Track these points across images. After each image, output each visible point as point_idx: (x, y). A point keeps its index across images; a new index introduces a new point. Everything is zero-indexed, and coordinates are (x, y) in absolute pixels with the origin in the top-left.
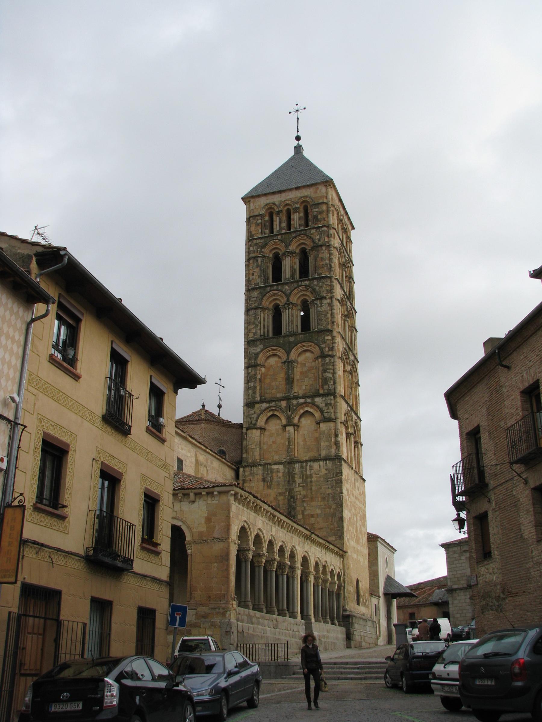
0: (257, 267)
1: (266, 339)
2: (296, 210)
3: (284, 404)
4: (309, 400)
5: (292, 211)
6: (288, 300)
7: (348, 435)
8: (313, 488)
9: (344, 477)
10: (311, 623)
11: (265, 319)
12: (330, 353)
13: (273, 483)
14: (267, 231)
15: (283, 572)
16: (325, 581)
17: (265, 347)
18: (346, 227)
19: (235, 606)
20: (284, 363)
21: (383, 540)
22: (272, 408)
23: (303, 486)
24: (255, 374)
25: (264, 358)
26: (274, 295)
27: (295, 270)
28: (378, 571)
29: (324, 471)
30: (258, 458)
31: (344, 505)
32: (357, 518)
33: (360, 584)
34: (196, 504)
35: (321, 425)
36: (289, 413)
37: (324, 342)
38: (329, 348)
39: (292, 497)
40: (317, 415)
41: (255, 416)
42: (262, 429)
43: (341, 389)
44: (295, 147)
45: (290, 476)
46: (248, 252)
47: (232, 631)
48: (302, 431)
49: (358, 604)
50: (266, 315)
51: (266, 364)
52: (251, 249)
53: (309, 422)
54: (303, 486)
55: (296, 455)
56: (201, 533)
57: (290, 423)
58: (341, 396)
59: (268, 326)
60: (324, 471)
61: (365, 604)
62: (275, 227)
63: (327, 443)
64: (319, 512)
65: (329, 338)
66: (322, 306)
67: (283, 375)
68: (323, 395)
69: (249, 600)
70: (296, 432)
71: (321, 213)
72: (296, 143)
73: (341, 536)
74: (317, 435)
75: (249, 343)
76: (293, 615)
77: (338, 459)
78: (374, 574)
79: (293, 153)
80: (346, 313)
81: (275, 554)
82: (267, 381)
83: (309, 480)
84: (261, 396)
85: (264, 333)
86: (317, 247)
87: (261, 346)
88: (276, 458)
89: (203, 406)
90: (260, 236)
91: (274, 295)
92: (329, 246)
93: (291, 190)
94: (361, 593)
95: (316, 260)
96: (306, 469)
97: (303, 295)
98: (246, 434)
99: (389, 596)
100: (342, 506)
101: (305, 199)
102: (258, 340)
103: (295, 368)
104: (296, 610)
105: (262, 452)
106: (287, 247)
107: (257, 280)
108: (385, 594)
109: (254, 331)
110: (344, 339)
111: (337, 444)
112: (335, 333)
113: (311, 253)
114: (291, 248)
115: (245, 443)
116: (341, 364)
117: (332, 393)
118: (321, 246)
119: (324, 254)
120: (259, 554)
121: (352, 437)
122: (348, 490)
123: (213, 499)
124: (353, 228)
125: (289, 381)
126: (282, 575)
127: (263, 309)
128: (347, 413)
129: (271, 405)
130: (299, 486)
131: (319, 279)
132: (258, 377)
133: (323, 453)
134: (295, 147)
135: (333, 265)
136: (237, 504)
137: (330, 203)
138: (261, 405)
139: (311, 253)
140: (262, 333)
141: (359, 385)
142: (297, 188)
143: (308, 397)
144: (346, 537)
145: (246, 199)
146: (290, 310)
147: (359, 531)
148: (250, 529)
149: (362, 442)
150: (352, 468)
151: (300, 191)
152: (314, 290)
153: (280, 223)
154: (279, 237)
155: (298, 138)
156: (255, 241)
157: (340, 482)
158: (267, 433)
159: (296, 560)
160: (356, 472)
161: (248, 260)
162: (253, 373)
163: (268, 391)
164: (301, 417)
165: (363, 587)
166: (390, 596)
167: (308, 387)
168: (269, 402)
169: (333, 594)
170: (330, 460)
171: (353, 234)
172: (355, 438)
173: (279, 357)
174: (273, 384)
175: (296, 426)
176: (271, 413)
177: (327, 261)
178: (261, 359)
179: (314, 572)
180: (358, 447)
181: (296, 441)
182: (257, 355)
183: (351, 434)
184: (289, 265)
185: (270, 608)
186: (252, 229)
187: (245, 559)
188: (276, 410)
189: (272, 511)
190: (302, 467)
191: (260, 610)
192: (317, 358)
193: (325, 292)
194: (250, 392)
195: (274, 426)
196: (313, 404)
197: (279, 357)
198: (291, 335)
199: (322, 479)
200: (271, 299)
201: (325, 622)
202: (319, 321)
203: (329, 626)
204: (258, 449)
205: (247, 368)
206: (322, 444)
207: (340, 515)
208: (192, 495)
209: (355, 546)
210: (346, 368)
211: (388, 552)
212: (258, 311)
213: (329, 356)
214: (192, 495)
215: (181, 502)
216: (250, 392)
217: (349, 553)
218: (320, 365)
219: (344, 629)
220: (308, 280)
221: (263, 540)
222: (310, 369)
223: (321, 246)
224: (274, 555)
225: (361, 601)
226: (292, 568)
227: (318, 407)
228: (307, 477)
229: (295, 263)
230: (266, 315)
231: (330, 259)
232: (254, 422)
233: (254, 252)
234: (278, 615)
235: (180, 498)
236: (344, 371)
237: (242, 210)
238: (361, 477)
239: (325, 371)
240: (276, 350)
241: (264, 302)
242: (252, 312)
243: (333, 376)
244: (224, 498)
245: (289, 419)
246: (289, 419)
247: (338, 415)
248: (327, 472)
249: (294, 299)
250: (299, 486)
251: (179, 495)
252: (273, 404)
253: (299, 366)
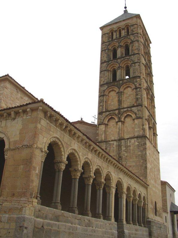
0: (105, 54)
1: (109, 83)
2: (123, 29)
3: (117, 112)
4: (129, 109)
5: (121, 30)
6: (119, 65)
7: (150, 128)
8: (131, 152)
9: (147, 146)
10: (123, 224)
11: (110, 75)
12: (139, 86)
13: (111, 150)
14: (110, 40)
15: (100, 188)
16: (134, 200)
17: (108, 87)
18: (147, 42)
19: (35, 204)
20: (117, 93)
21: (169, 184)
23: (126, 151)
25: (108, 92)
26: (113, 64)
27: (123, 53)
28: (166, 200)
29: (137, 143)
30: (103, 138)
31: (147, 160)
32: (155, 169)
33: (157, 205)
34: (16, 120)
35: (135, 120)
36: (119, 116)
37: (136, 82)
38: (139, 84)
39: (120, 157)
40: (134, 116)
41: (103, 118)
42: (106, 125)
43: (145, 103)
44: (124, 11)
45: (119, 146)
46: (102, 48)
47: (25, 226)
48: (126, 124)
49: (156, 215)
50: (109, 74)
51: (109, 95)
52: (103, 47)
53: (129, 120)
54: (126, 151)
55: (123, 136)
56: (15, 142)
57: (120, 121)
58: (145, 107)
59: (110, 78)
60: (137, 143)
61: (160, 216)
62: (114, 37)
63: (138, 129)
64: (134, 164)
65: (139, 80)
66: (135, 66)
67: (117, 99)
68: (137, 106)
69: (59, 202)
70: (123, 125)
71: (134, 28)
72: (125, 9)
73: (146, 177)
74: (133, 126)
75: (101, 86)
76: (106, 217)
77: (144, 137)
78: (164, 201)
79: (123, 13)
80: (148, 73)
81: (92, 173)
82: (109, 102)
83: (129, 148)
84: (106, 110)
85: (108, 81)
86: (132, 42)
87: (107, 87)
88: (113, 138)
89: (82, 119)
90: (107, 41)
91: (113, 64)
92: (138, 41)
93: (120, 21)
94: (158, 209)
95: (132, 47)
96: (127, 142)
97: (127, 63)
98: (98, 127)
99: (173, 213)
100: (146, 161)
101: (126, 24)
102: (105, 84)
103: (122, 95)
104: (110, 215)
105: (106, 136)
106: (119, 44)
107: (105, 59)
108: (171, 212)
109: (103, 80)
110: (147, 82)
111: (144, 130)
112: (142, 78)
113: (130, 45)
114: (120, 44)
115: (97, 132)
116: (145, 92)
117: (141, 105)
118: (135, 41)
119: (136, 44)
120: (75, 169)
121: (152, 130)
122: (149, 154)
123: (27, 115)
124: (151, 43)
125: (120, 102)
126: (100, 190)
127: (108, 71)
128: (149, 116)
129: (110, 113)
130: (124, 151)
131: (134, 54)
132: (105, 100)
133: (136, 134)
134: (124, 11)
135: (140, 49)
136: (48, 122)
137: (139, 24)
139: (130, 45)
140: (107, 81)
141: (155, 108)
142: (124, 20)
143: (129, 107)
144: (149, 178)
145: (102, 28)
146: (120, 70)
147: (156, 177)
148: (63, 146)
149: (157, 134)
150: (152, 144)
151: (125, 21)
152: (132, 60)
153: (116, 35)
154: (116, 40)
155: (125, 8)
156: (105, 44)
157: (145, 149)
158: (108, 127)
159: (112, 182)
160: (154, 146)
161: (102, 51)
163: (109, 107)
164: (125, 117)
165: (159, 206)
166: (173, 213)
167: (129, 103)
168: (109, 111)
169: (141, 208)
170: (139, 137)
171: (151, 45)
172: (153, 130)
173: (115, 91)
174: (112, 103)
175: (123, 123)
176: (111, 117)
177: (138, 48)
178: (106, 93)
179: (126, 192)
180: (155, 136)
181: (123, 129)
182: (104, 91)
183: (151, 127)
184: (120, 52)
185: (86, 211)
186: (104, 39)
187: (58, 169)
188: (113, 115)
189: (88, 140)
190: (125, 142)
191: (73, 212)
192: (133, 90)
193: (137, 60)
194: (101, 107)
195: (112, 123)
196: (131, 111)
197: (115, 91)
198: (121, 80)
199: (136, 147)
200: (112, 66)
201: (134, 224)
202: (134, 73)
203: (138, 227)
204: (104, 134)
205: (100, 96)
206: (136, 130)
207: (145, 166)
208: (12, 113)
209: (154, 184)
210: (148, 97)
211: (171, 192)
212: (106, 72)
213: (139, 88)
214: (12, 113)
215: (6, 120)
216: (101, 107)
217: (150, 186)
218: (135, 92)
219: (147, 229)
220: (129, 56)
221: (78, 159)
222: (130, 95)
223: (135, 41)
224: (90, 174)
225: (158, 213)
226: (107, 186)
227: (134, 112)
228: (128, 147)
229: (123, 51)
230: (109, 74)
231: (139, 46)
232: (102, 121)
233: (104, 48)
234: (92, 217)
235: (5, 116)
236: (147, 98)
237: (100, 33)
238: (157, 150)
239: (137, 95)
240: (114, 88)
241: (108, 68)
242: (102, 73)
243: (141, 96)
244: (35, 114)
245: (119, 118)
246: (119, 118)
247: (144, 115)
248: (138, 143)
249: (122, 65)
250: (124, 151)
251: (4, 114)
252: (111, 112)
253: (125, 94)
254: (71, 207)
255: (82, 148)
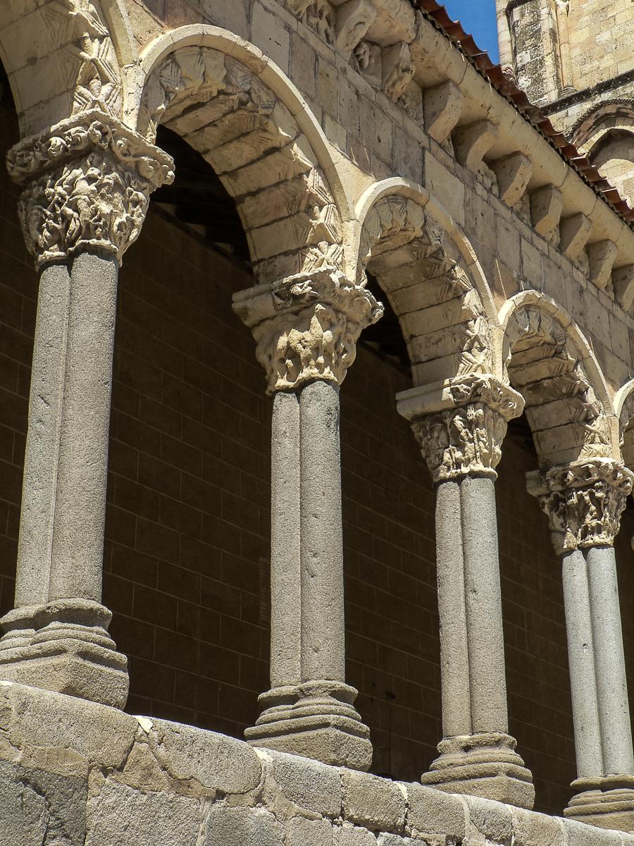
22: (601, 112)
24: (537, 21)
138: (563, 113)
162: (528, 19)
188: (620, 115)
254: (288, 690)
255: (347, 92)
